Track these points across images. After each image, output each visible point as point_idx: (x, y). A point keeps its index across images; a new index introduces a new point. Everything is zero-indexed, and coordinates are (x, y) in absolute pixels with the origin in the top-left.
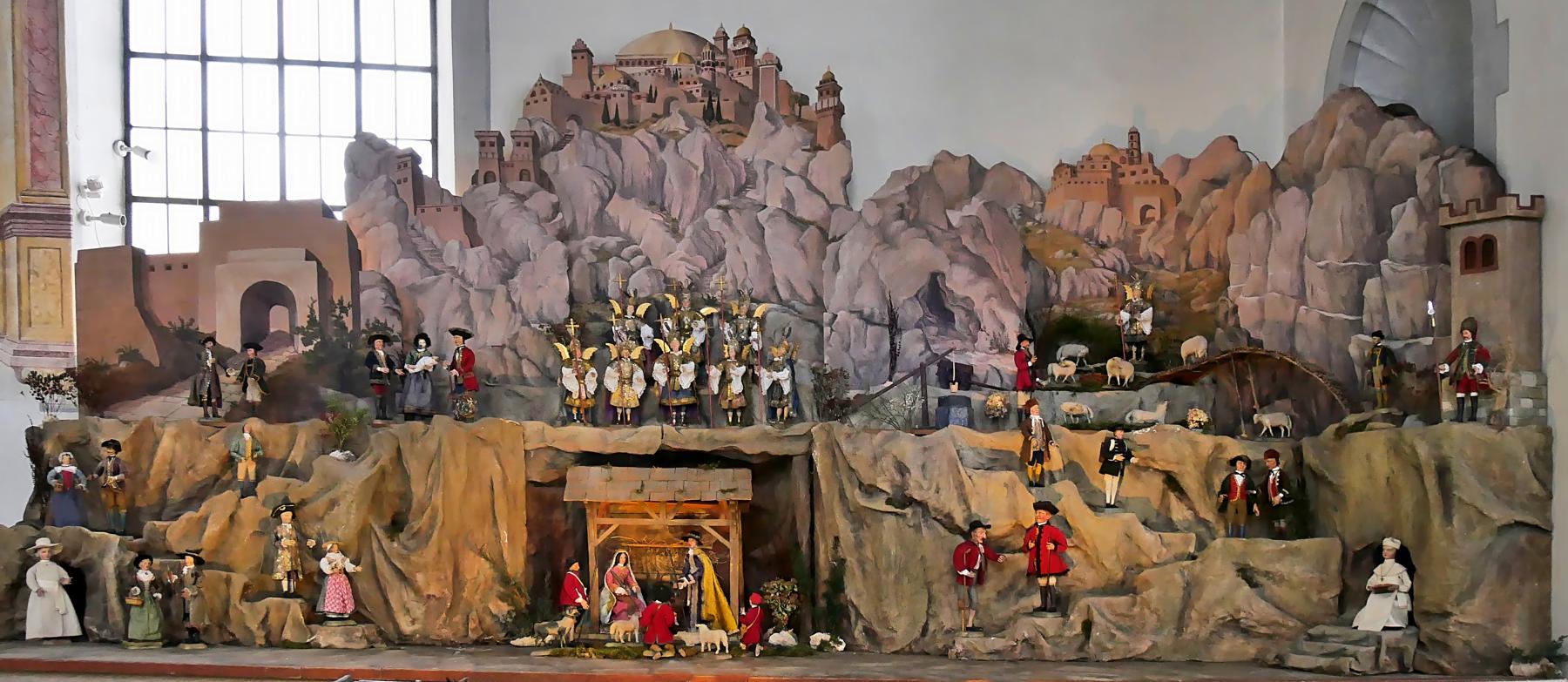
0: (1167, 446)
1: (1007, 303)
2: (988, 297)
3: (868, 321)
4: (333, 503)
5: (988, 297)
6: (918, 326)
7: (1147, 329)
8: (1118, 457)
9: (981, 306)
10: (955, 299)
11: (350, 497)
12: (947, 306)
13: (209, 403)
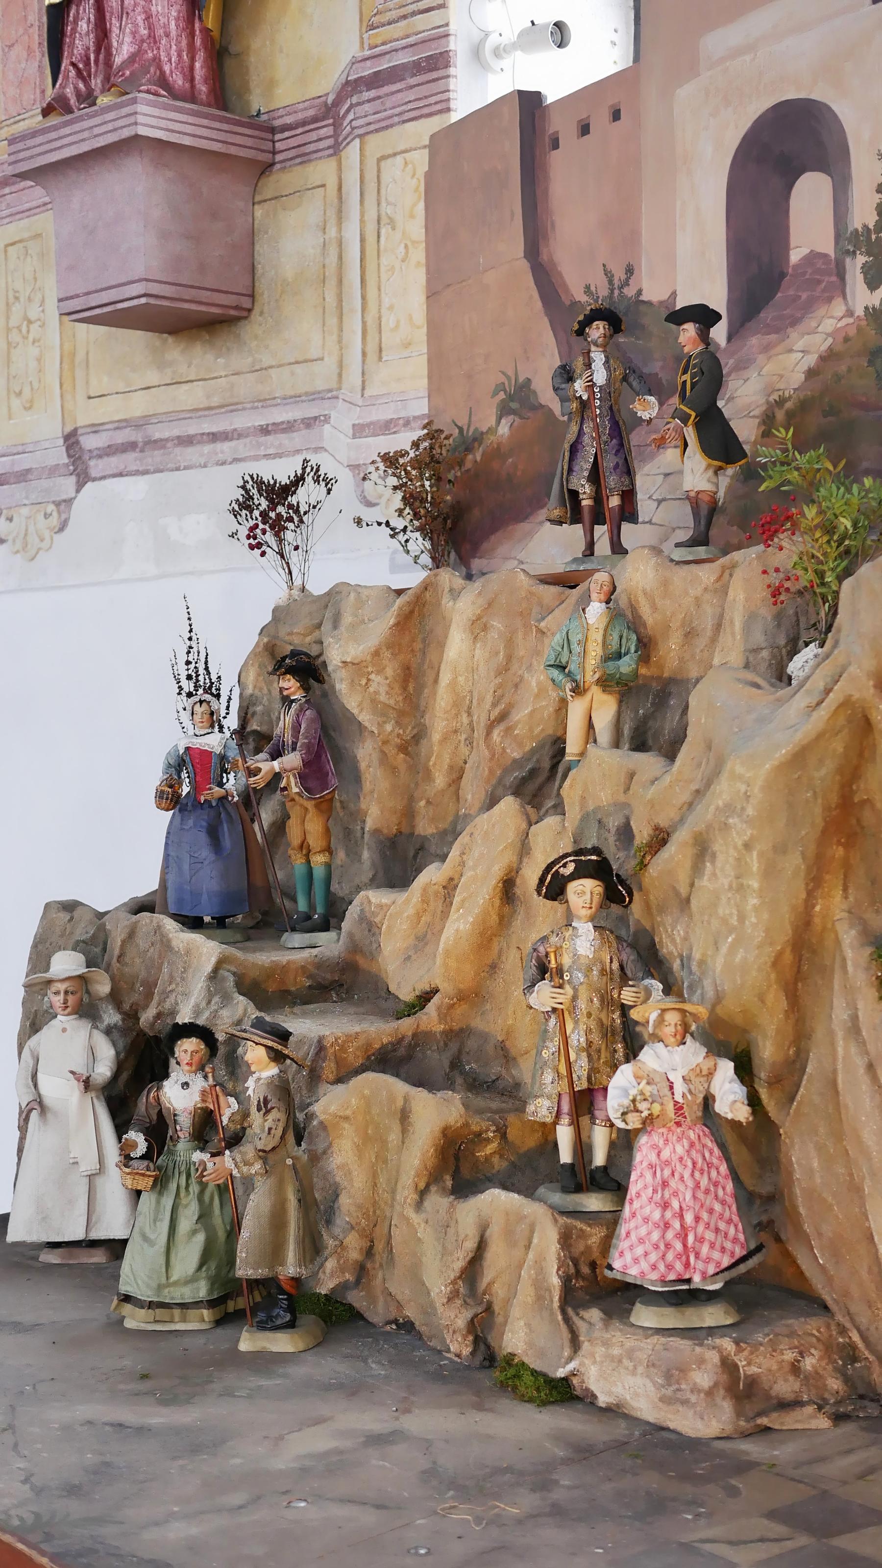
4: (702, 850)
11: (740, 831)
13: (598, 517)
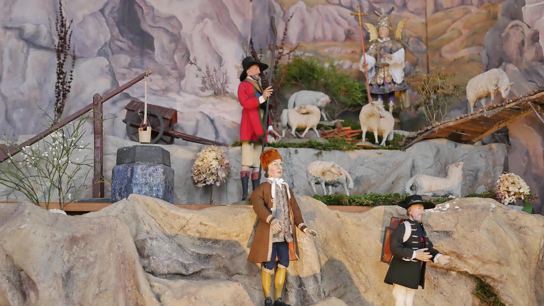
0: (482, 235)
1: (225, 25)
2: (201, 18)
3: (31, 42)
5: (201, 18)
6: (102, 53)
7: (398, 76)
8: (419, 254)
9: (189, 29)
10: (154, 18)
12: (145, 27)
